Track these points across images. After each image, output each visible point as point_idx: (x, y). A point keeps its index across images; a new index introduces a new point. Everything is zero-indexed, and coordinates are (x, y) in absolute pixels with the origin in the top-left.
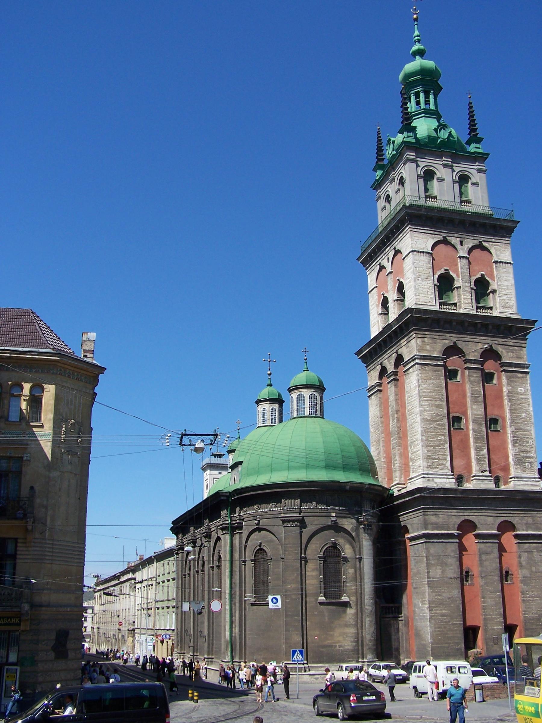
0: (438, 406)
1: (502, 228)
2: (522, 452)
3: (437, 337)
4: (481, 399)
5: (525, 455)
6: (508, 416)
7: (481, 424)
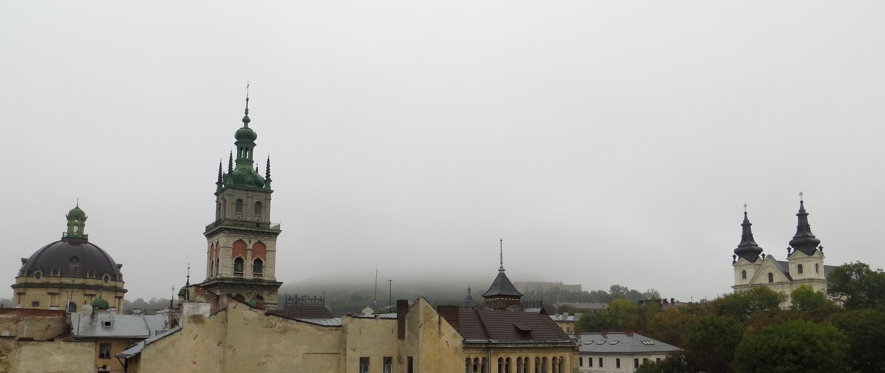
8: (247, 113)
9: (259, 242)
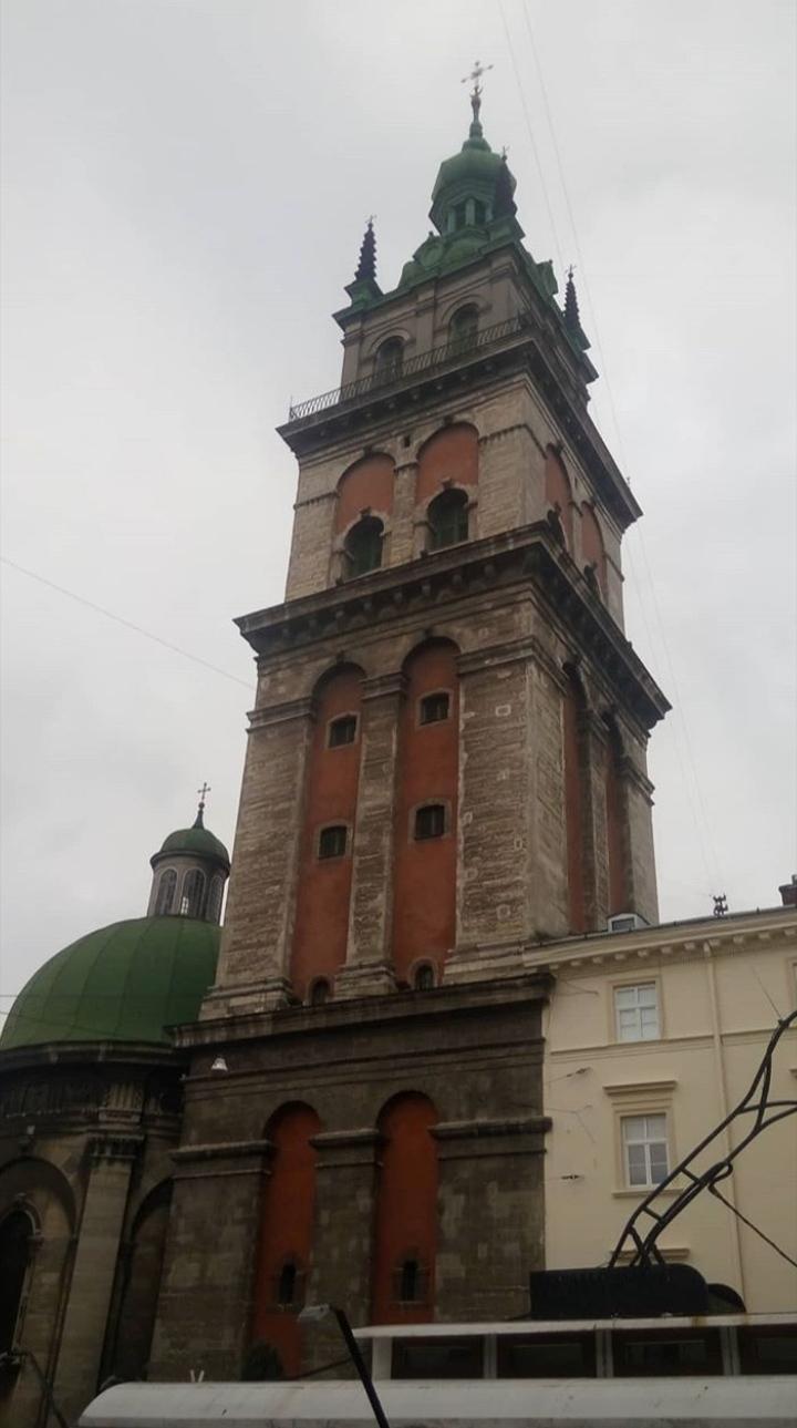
0: (280, 816)
2: (490, 876)
3: (306, 659)
4: (388, 767)
5: (498, 882)
6: (461, 784)
7: (379, 831)
9: (450, 426)
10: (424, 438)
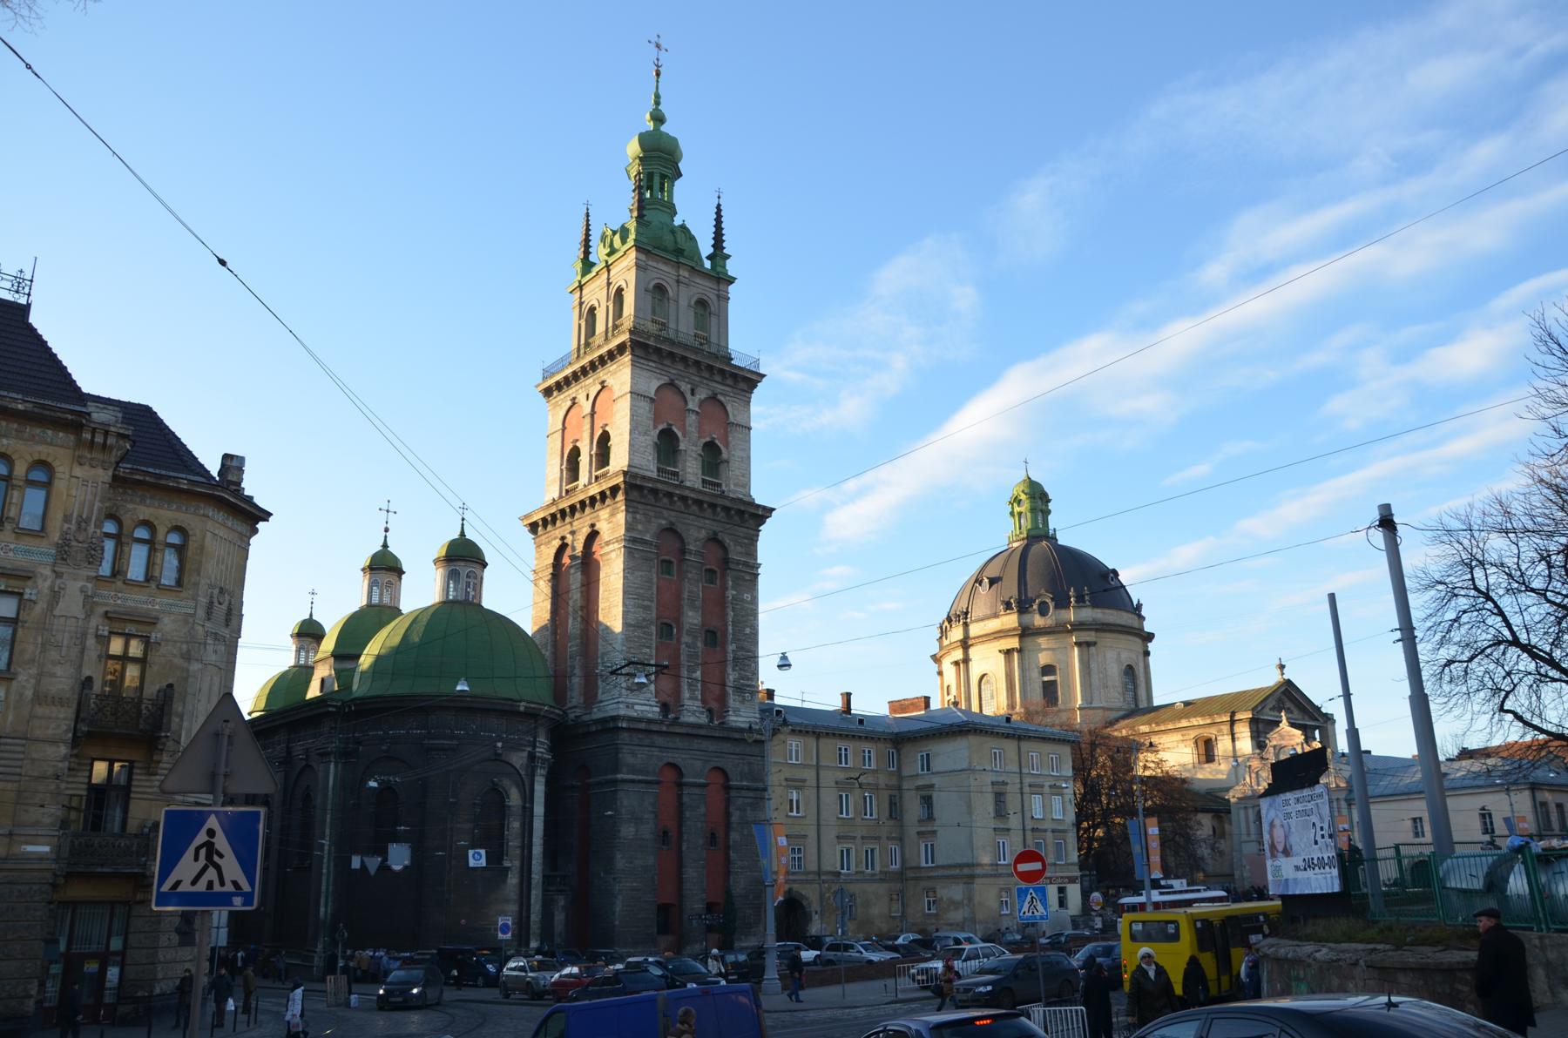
1: (746, 379)
8: (657, 103)
10: (703, 396)
